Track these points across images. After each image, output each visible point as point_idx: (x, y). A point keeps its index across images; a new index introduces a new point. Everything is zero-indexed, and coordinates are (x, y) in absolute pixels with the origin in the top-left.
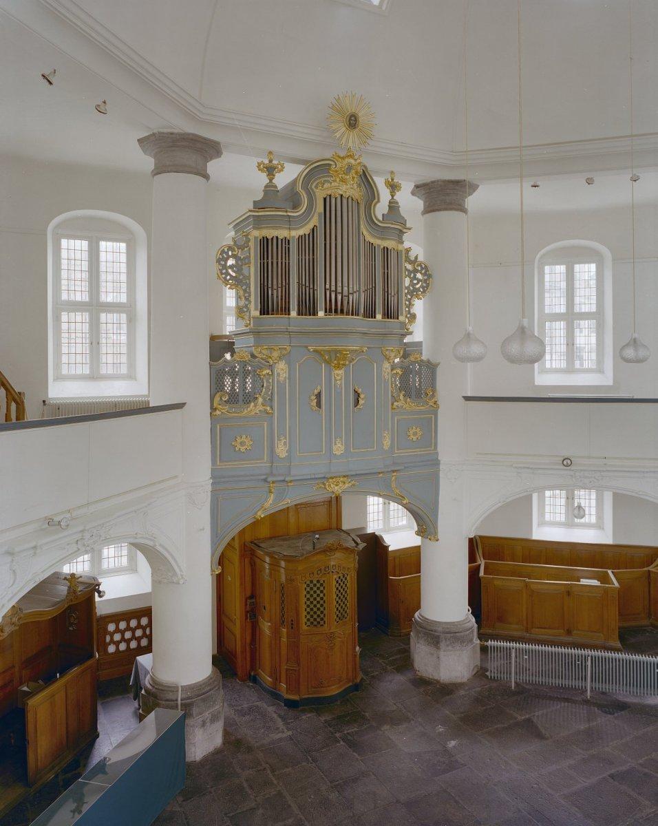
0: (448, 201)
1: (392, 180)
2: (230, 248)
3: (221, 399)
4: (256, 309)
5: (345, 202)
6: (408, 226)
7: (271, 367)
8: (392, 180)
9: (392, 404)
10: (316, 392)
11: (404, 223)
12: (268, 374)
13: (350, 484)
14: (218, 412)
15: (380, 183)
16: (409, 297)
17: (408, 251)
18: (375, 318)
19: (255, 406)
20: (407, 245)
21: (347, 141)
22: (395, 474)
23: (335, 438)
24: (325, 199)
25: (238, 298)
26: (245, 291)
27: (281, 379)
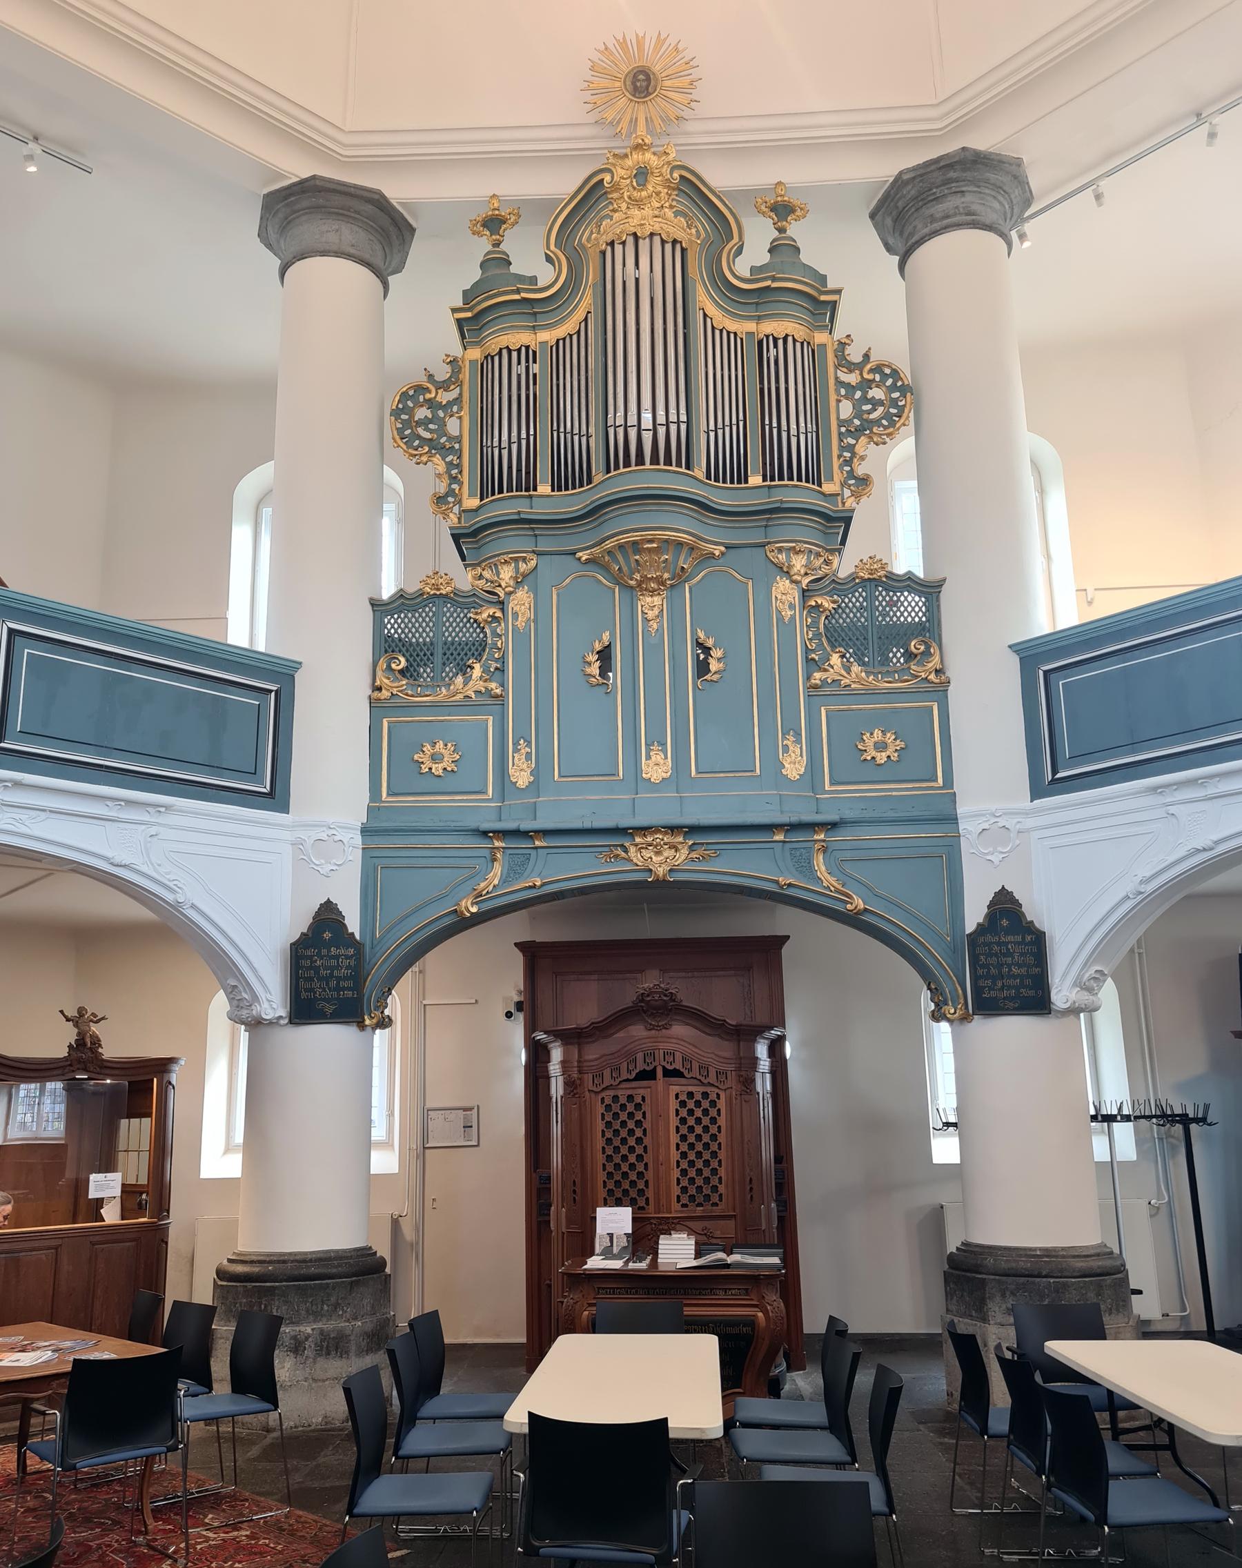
2: (420, 389)
3: (389, 667)
4: (471, 495)
6: (831, 285)
10: (598, 647)
14: (385, 694)
17: (842, 345)
18: (746, 482)
19: (465, 683)
20: (839, 334)
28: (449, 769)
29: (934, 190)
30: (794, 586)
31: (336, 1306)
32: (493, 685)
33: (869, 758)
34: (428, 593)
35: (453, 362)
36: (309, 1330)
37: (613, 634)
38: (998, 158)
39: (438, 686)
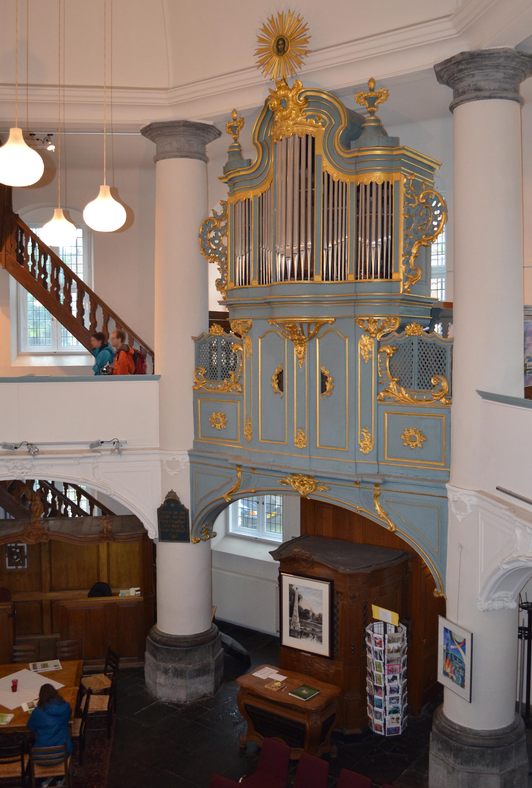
29: (456, 75)
30: (372, 340)
31: (180, 659)
34: (214, 335)
35: (224, 204)
36: (170, 666)
38: (488, 52)
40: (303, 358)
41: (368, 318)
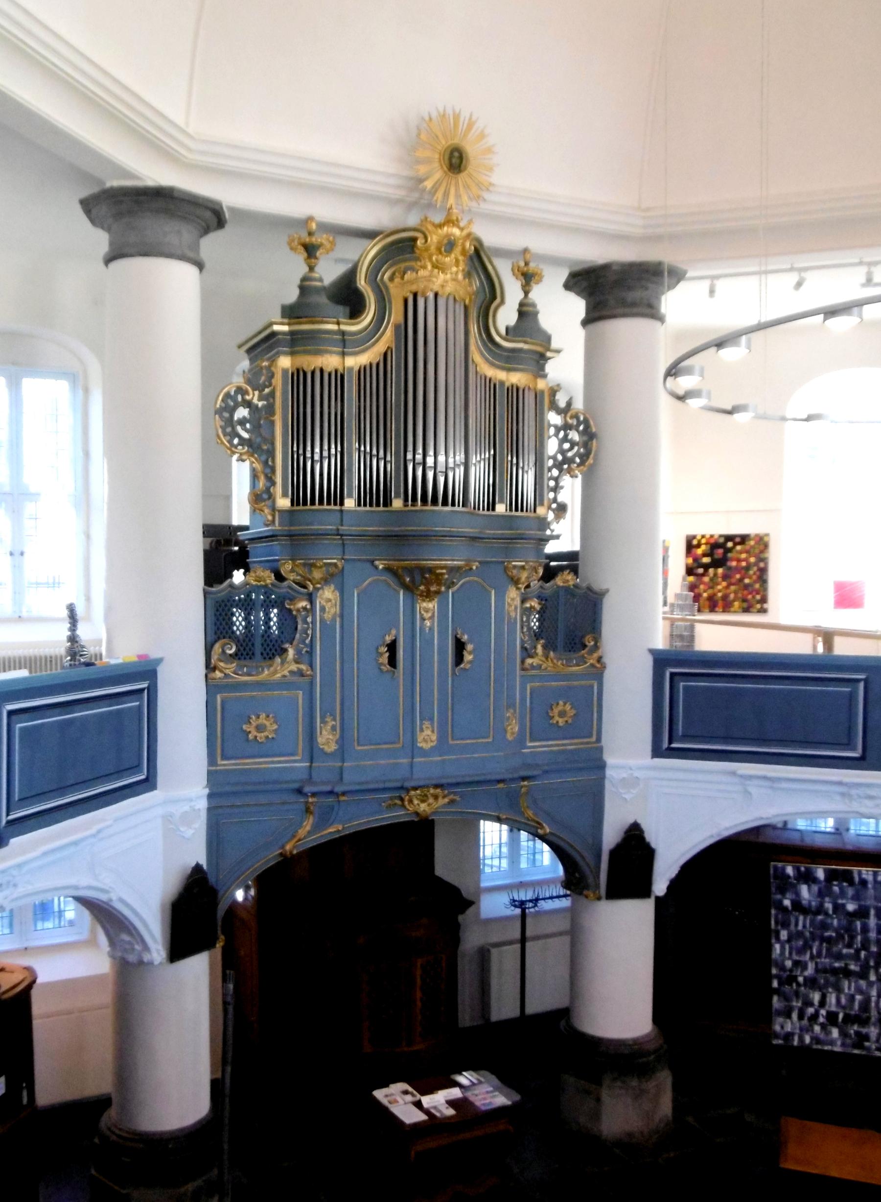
0: (629, 300)
1: (527, 264)
3: (224, 652)
4: (285, 495)
5: (441, 302)
7: (311, 598)
8: (527, 264)
9: (523, 662)
10: (388, 639)
11: (547, 339)
12: (305, 608)
13: (446, 800)
14: (218, 674)
15: (504, 270)
16: (555, 472)
17: (553, 392)
18: (494, 509)
19: (283, 663)
21: (446, 195)
22: (526, 783)
23: (421, 720)
24: (406, 301)
25: (254, 476)
26: (266, 463)
27: (328, 616)
28: (270, 737)
32: (303, 667)
33: (555, 722)
37: (398, 631)
39: (261, 666)
40: (432, 618)
41: (523, 563)
